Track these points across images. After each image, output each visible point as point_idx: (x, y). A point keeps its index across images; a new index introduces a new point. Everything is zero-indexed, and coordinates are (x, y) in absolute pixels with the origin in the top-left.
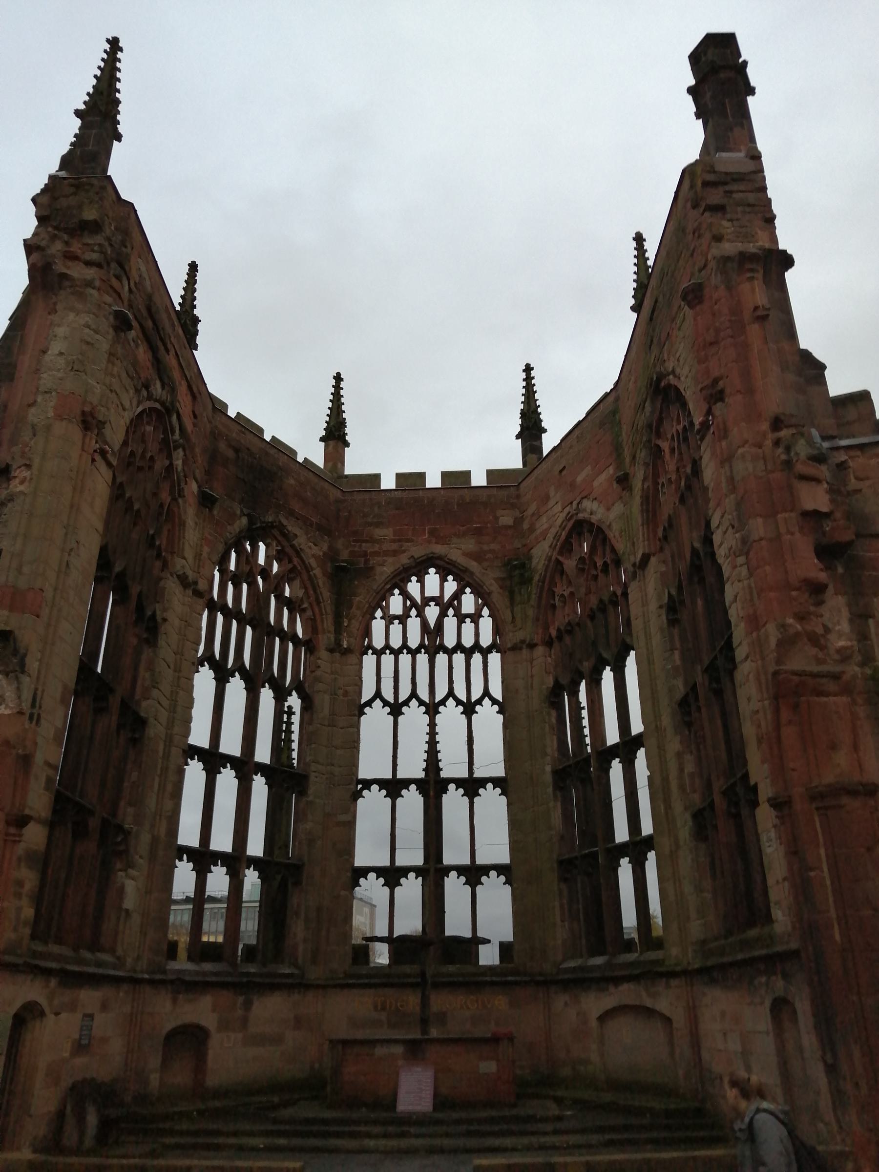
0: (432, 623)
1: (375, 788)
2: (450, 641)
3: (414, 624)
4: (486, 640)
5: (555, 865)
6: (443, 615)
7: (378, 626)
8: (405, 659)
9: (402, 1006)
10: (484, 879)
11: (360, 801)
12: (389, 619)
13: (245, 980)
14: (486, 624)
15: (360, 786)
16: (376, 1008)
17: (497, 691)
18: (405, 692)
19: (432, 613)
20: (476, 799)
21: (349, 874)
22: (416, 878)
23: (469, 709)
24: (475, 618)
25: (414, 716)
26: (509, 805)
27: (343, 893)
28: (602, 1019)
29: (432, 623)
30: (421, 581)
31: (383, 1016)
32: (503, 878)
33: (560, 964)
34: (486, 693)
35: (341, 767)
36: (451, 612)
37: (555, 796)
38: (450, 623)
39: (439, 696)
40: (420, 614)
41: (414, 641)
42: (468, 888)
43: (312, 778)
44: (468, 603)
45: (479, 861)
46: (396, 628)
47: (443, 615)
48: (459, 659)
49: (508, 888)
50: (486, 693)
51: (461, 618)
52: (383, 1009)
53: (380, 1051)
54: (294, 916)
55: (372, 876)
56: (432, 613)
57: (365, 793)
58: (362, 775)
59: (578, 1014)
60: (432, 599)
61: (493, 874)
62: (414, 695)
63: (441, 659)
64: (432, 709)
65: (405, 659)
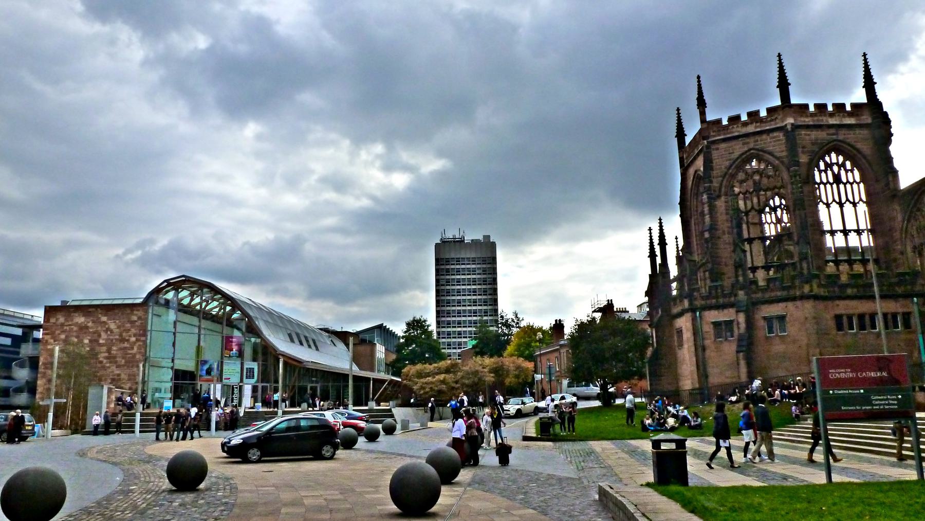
0: (836, 173)
2: (844, 180)
3: (829, 173)
4: (858, 179)
6: (840, 169)
7: (817, 173)
8: (828, 186)
12: (820, 171)
14: (856, 172)
17: (864, 199)
18: (830, 200)
19: (836, 169)
23: (854, 204)
24: (852, 171)
25: (835, 207)
29: (836, 173)
30: (830, 156)
34: (861, 200)
36: (842, 168)
38: (843, 172)
39: (843, 202)
40: (832, 170)
41: (831, 180)
44: (848, 165)
46: (823, 174)
47: (840, 169)
48: (848, 186)
50: (861, 200)
51: (847, 171)
56: (836, 169)
60: (835, 163)
62: (834, 200)
63: (842, 186)
64: (841, 205)
65: (828, 186)
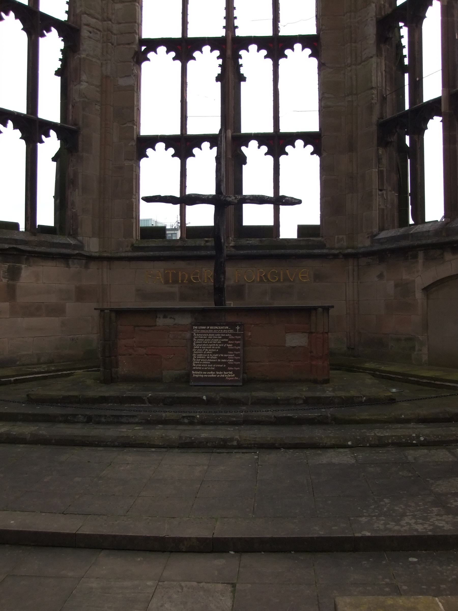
1: (162, 49)
5: (374, 128)
9: (195, 279)
10: (288, 149)
11: (145, 65)
13: (6, 246)
15: (143, 48)
16: (167, 282)
20: (282, 61)
21: (134, 143)
22: (211, 148)
26: (321, 67)
27: (127, 163)
28: (427, 290)
31: (175, 289)
32: (310, 148)
33: (376, 235)
35: (120, 23)
37: (379, 50)
42: (270, 159)
43: (85, 32)
45: (284, 128)
49: (316, 158)
52: (175, 281)
53: (161, 321)
54: (71, 186)
55: (160, 146)
57: (151, 55)
58: (145, 35)
59: (396, 286)
61: (299, 143)
